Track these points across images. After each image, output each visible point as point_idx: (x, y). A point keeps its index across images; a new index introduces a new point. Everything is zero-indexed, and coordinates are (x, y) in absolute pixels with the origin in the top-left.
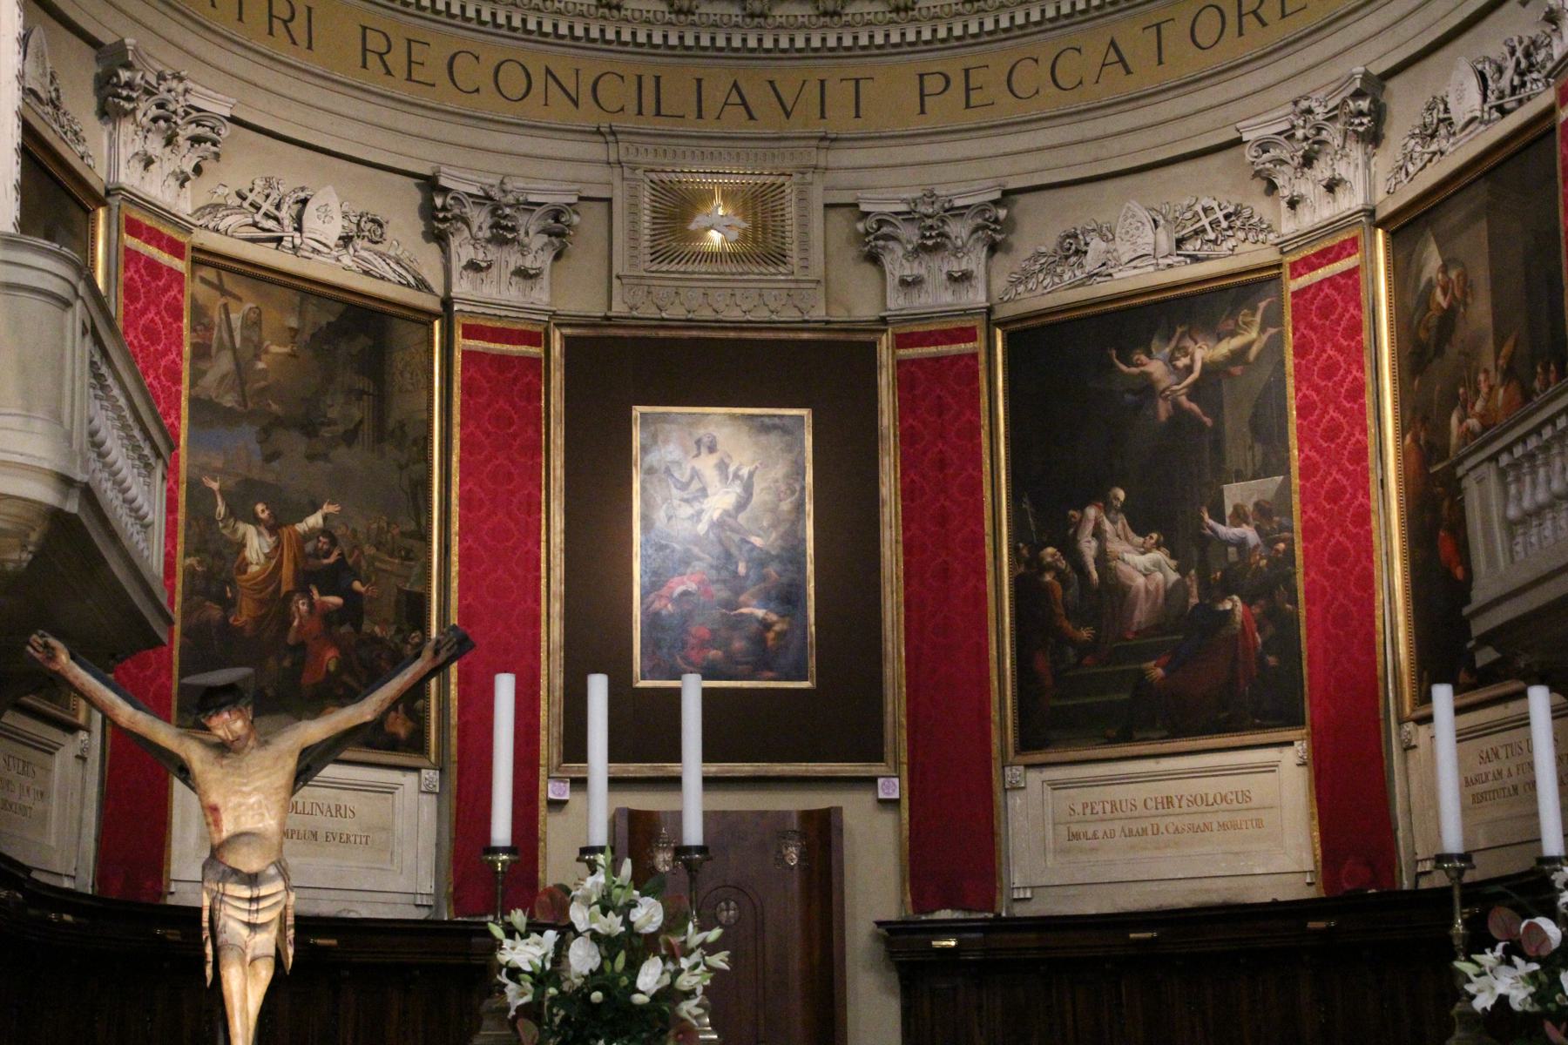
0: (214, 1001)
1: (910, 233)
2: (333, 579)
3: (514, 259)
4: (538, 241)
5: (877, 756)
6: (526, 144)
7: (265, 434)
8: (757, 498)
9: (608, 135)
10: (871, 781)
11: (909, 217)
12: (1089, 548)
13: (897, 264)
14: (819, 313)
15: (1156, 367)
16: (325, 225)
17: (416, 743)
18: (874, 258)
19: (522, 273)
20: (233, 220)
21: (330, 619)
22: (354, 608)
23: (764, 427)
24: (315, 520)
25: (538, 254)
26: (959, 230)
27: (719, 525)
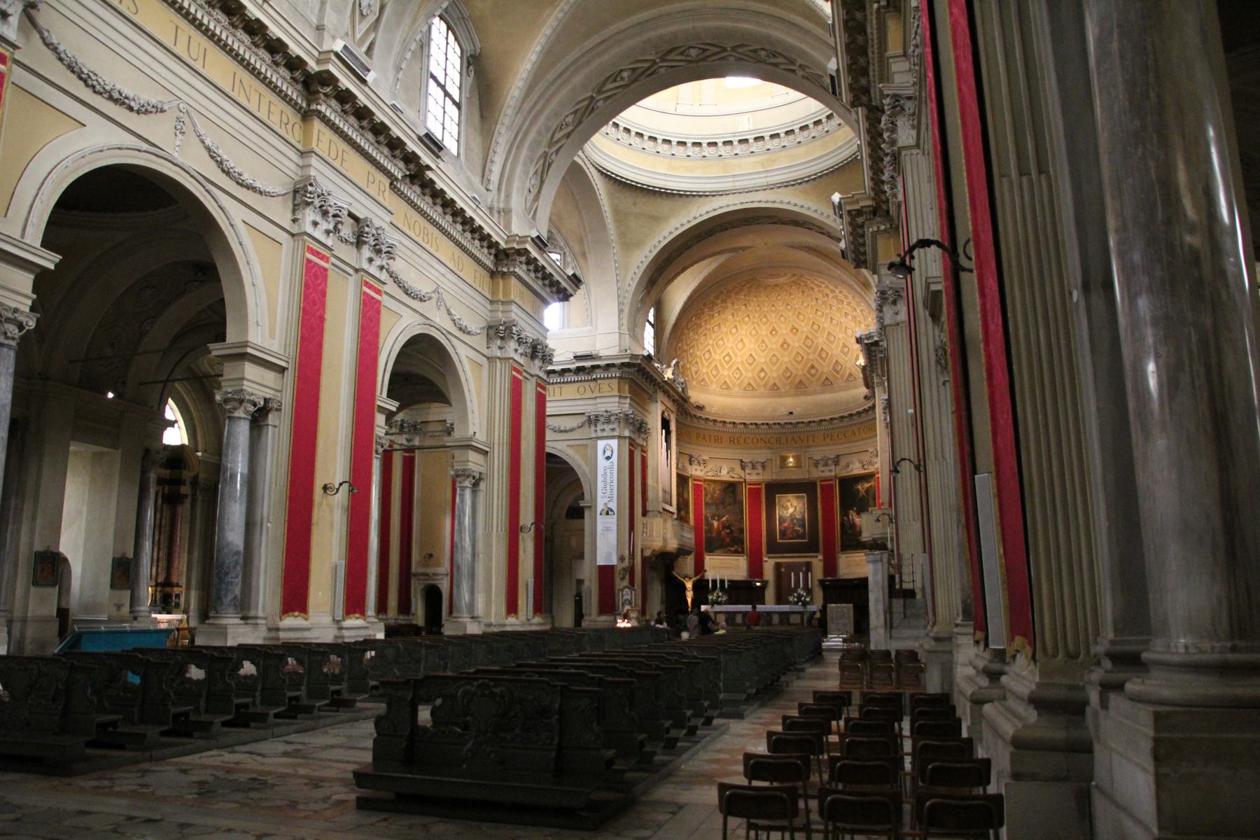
0: (687, 602)
1: (822, 462)
2: (728, 527)
3: (756, 472)
4: (760, 468)
5: (817, 551)
6: (757, 451)
7: (716, 506)
8: (798, 509)
9: (771, 449)
10: (817, 557)
11: (822, 460)
12: (851, 517)
13: (821, 468)
14: (807, 477)
15: (860, 487)
16: (724, 471)
17: (743, 552)
18: (817, 467)
19: (757, 474)
20: (710, 474)
21: (728, 534)
22: (732, 532)
23: (798, 497)
24: (725, 518)
25: (760, 470)
26: (830, 462)
27: (791, 515)
